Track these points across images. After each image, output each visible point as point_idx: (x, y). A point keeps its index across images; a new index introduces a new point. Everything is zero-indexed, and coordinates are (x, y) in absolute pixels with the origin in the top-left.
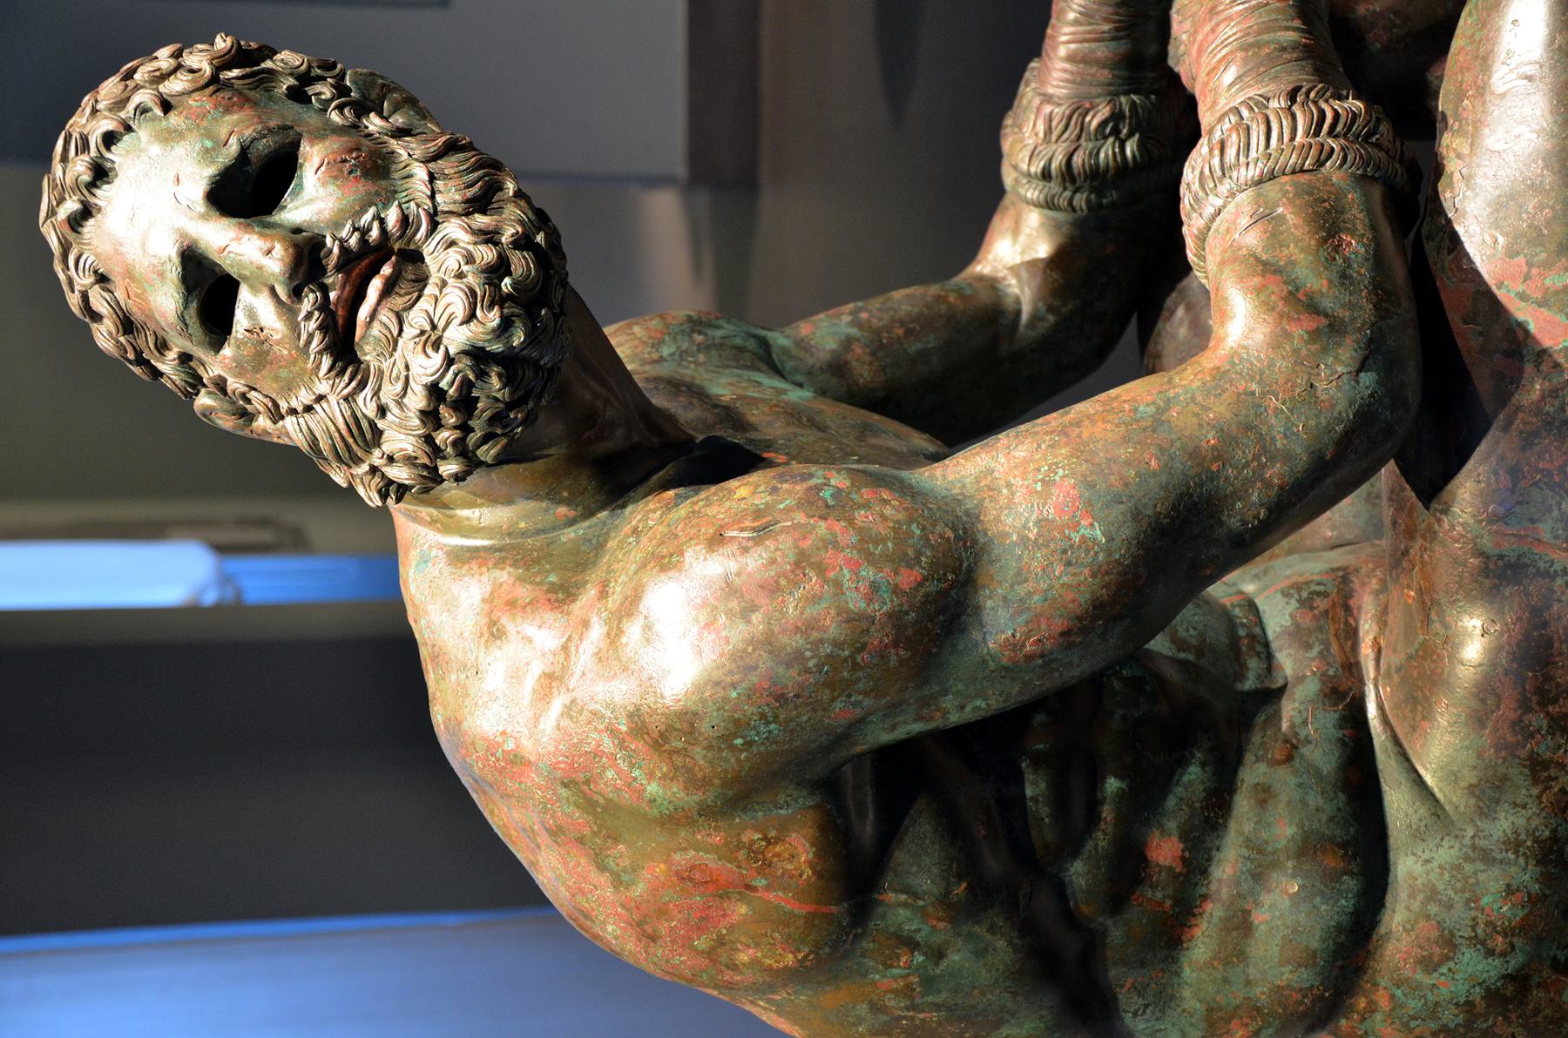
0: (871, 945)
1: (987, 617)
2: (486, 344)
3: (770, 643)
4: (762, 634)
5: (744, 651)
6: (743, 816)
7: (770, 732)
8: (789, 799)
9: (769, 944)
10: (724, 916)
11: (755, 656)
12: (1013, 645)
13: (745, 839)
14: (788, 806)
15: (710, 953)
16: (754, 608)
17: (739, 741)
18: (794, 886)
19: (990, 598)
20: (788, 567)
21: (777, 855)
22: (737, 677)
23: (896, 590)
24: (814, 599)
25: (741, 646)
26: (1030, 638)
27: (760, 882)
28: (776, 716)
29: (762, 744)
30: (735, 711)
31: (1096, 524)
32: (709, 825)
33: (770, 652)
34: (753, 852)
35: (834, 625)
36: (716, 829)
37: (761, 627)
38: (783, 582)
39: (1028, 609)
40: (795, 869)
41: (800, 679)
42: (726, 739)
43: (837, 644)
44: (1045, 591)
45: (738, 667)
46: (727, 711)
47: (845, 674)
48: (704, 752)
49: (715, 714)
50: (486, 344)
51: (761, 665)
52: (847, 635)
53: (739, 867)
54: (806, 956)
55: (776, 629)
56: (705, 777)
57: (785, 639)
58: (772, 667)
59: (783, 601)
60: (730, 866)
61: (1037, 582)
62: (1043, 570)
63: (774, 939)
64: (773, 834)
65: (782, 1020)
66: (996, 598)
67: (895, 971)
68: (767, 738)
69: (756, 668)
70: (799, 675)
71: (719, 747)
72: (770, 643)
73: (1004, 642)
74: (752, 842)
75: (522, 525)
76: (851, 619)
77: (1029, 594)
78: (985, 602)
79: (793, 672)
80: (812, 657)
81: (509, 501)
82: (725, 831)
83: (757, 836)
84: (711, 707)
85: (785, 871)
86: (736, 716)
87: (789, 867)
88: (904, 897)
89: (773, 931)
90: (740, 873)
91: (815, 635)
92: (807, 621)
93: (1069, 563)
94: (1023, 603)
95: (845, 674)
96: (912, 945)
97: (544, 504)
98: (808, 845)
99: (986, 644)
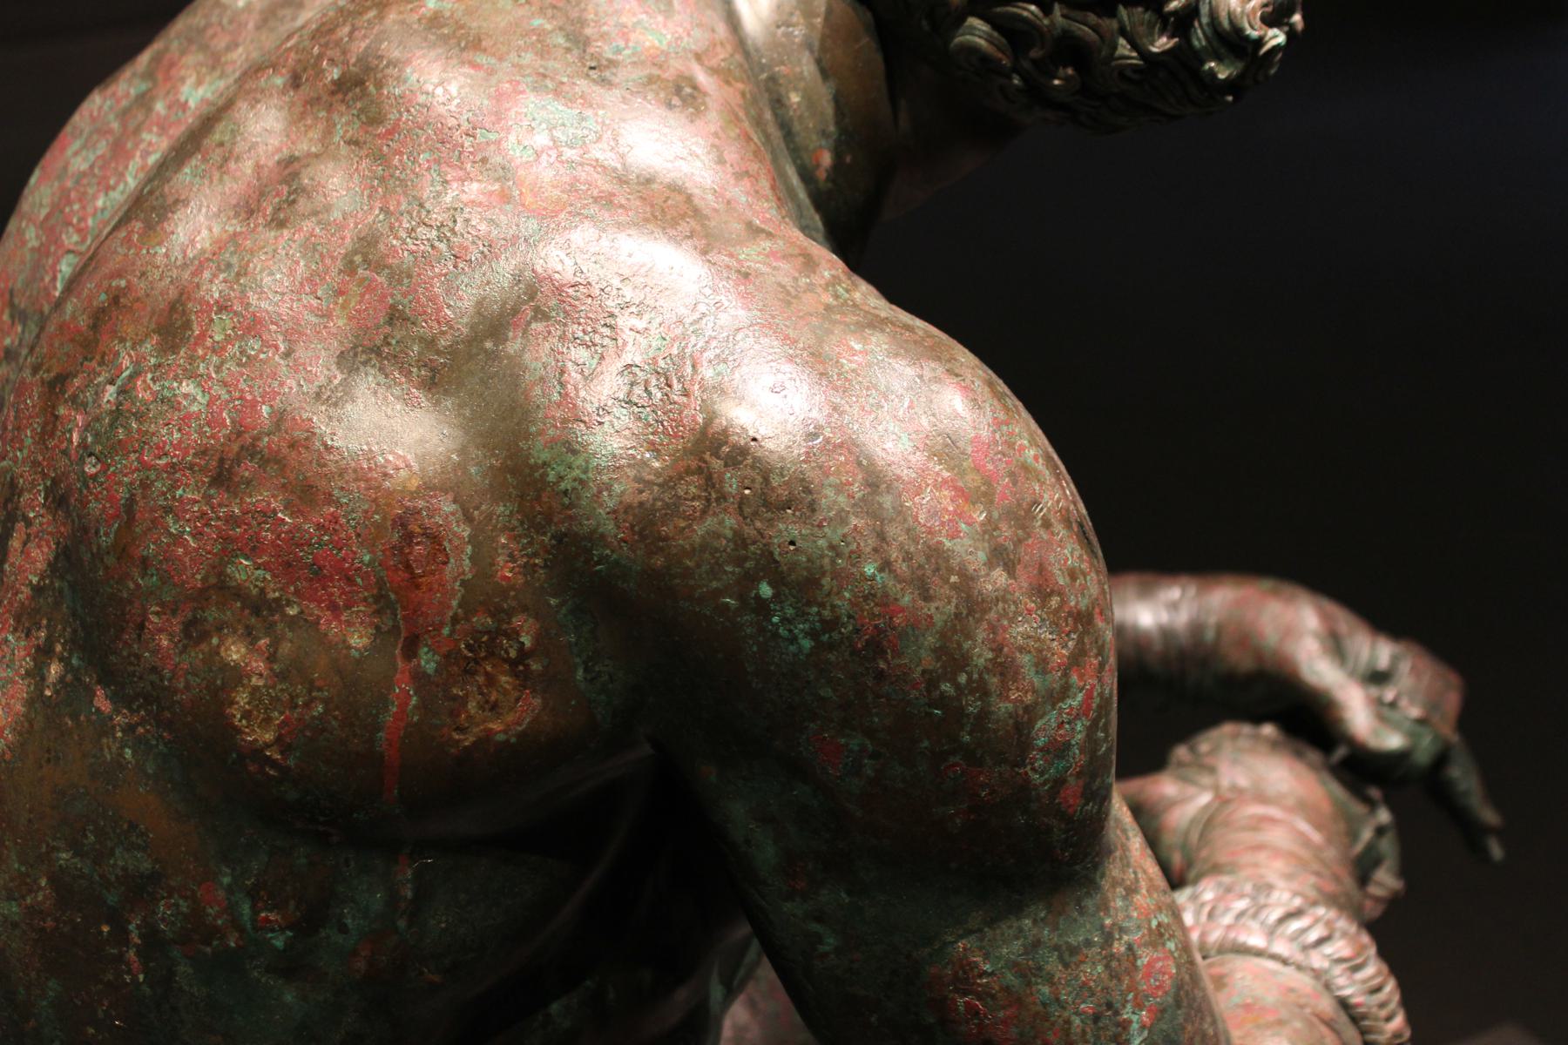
0: (303, 861)
1: (1006, 928)
2: (1205, 20)
3: (971, 612)
4: (980, 593)
5: (950, 571)
6: (564, 610)
7: (793, 640)
8: (605, 678)
9: (292, 698)
10: (334, 608)
11: (946, 591)
12: (965, 977)
13: (517, 621)
14: (592, 679)
15: (222, 588)
16: (1010, 569)
17: (766, 590)
18: (436, 721)
19: (1035, 922)
20: (1073, 604)
21: (491, 681)
22: (902, 567)
23: (1059, 782)
24: (1042, 665)
25: (954, 563)
26: (979, 999)
27: (428, 661)
28: (831, 646)
29: (762, 630)
30: (836, 575)
31: (1146, 1033)
32: (535, 555)
33: (957, 616)
34: (492, 640)
35: (1010, 706)
36: (529, 569)
37: (990, 587)
38: (1054, 602)
39: (1029, 984)
40: (469, 717)
41: (917, 675)
42: (769, 566)
43: (984, 715)
44: (1058, 1000)
45: (921, 567)
46: (833, 562)
47: (926, 744)
48: (729, 533)
49: (821, 542)
50: (1205, 20)
51: (933, 605)
52: (996, 731)
53: (455, 620)
54: (273, 763)
55: (992, 615)
56: (666, 539)
57: (981, 634)
58: (933, 624)
59: (1030, 612)
60: (455, 603)
61: (1068, 983)
62: (1084, 984)
63: (307, 705)
64: (535, 666)
65: (19, 707)
66: (1035, 931)
67: (246, 909)
68: (776, 635)
69: (927, 598)
70: (924, 672)
71: (746, 558)
72: (971, 612)
73: (969, 964)
74: (514, 635)
75: (795, 98)
76: (1022, 726)
77: (1050, 980)
78: (1027, 917)
79: (928, 661)
80: (957, 686)
81: (825, 73)
82: (526, 582)
83: (527, 640)
84: (834, 534)
85: (463, 701)
86: (826, 581)
87: (472, 706)
88: (409, 894)
89: (326, 702)
90: (442, 625)
91: (993, 681)
92: (1014, 660)
93: (1096, 1018)
94: (1029, 973)
95: (926, 744)
96: (309, 922)
97: (832, 128)
98: (520, 729)
99: (961, 937)
